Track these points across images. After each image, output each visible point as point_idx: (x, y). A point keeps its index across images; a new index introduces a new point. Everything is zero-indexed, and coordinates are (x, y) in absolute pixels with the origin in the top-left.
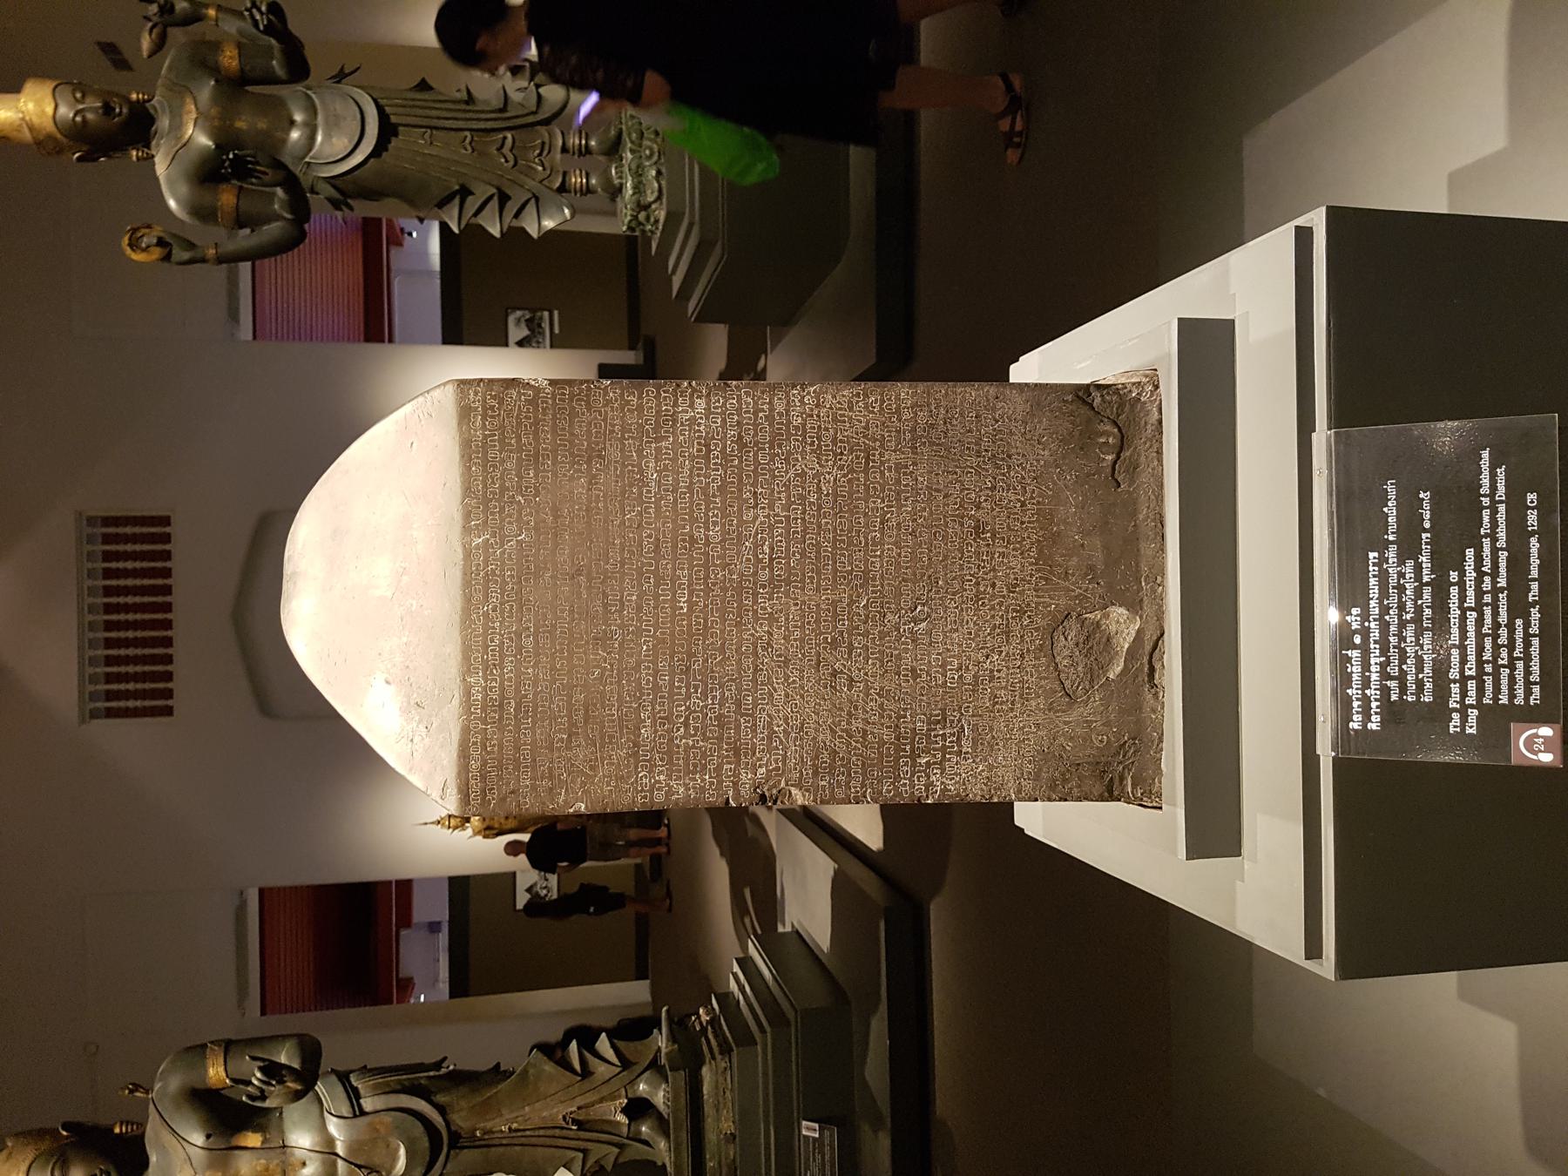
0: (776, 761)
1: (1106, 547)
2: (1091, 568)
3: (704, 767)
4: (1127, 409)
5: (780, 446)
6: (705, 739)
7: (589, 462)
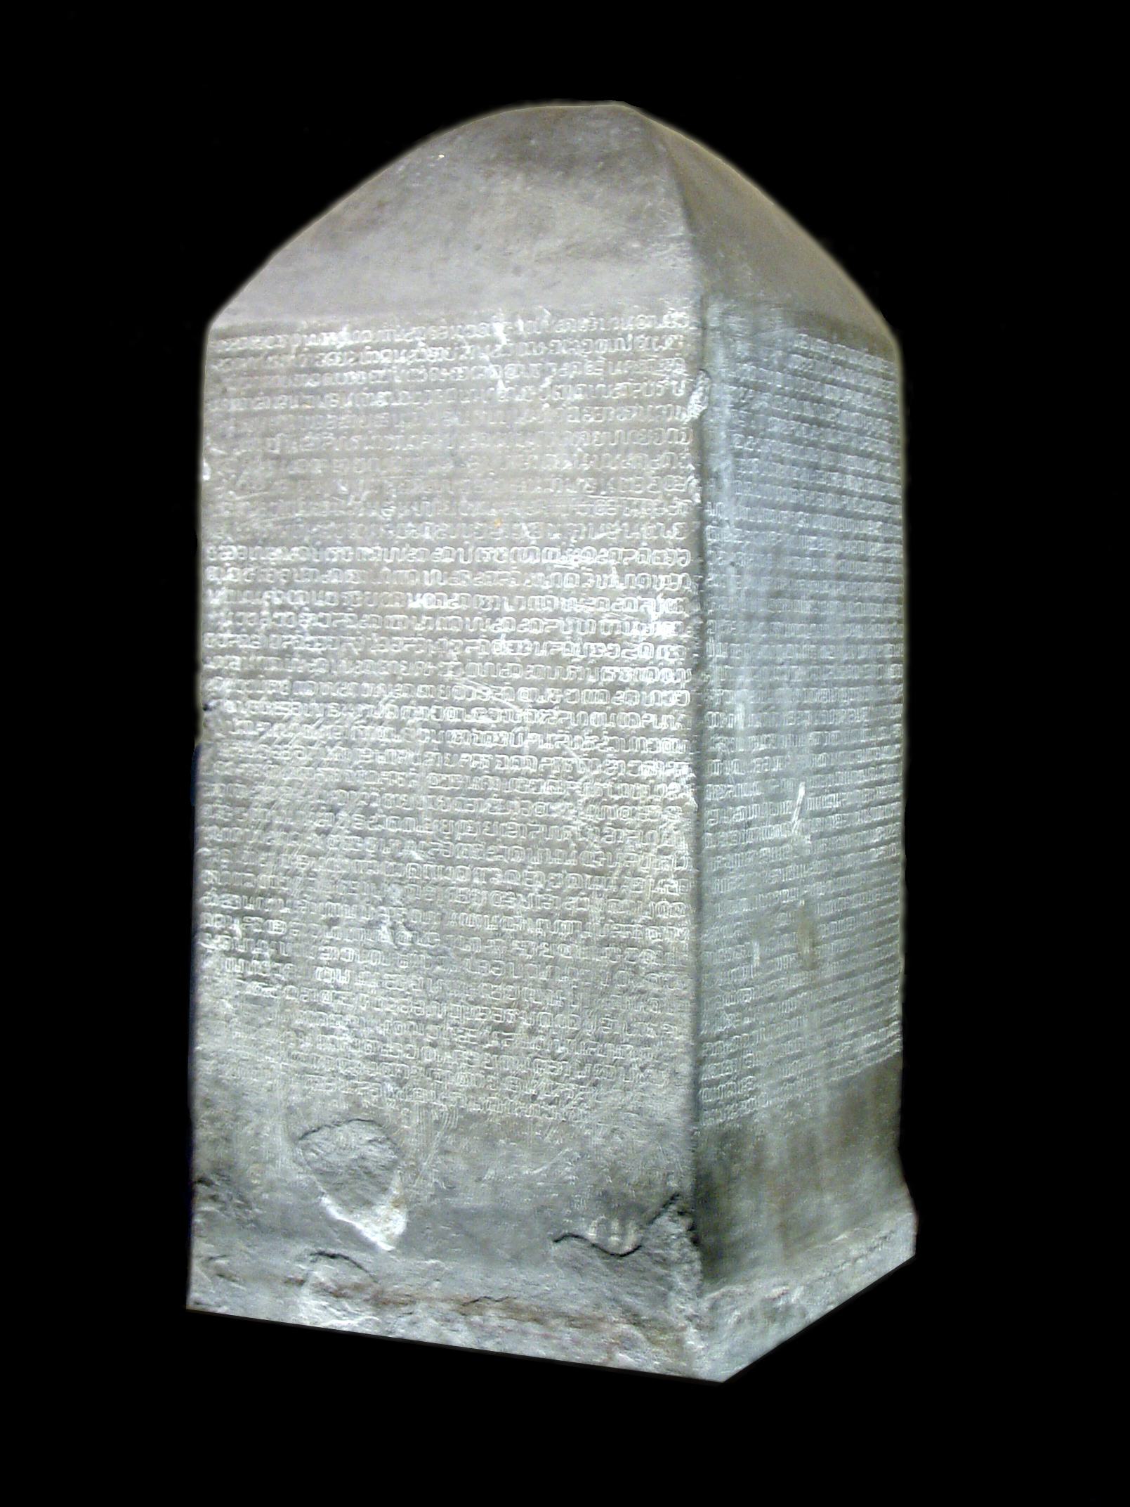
1: (476, 1214)
2: (452, 1190)
3: (237, 630)
4: (660, 1270)
5: (611, 744)
7: (591, 473)
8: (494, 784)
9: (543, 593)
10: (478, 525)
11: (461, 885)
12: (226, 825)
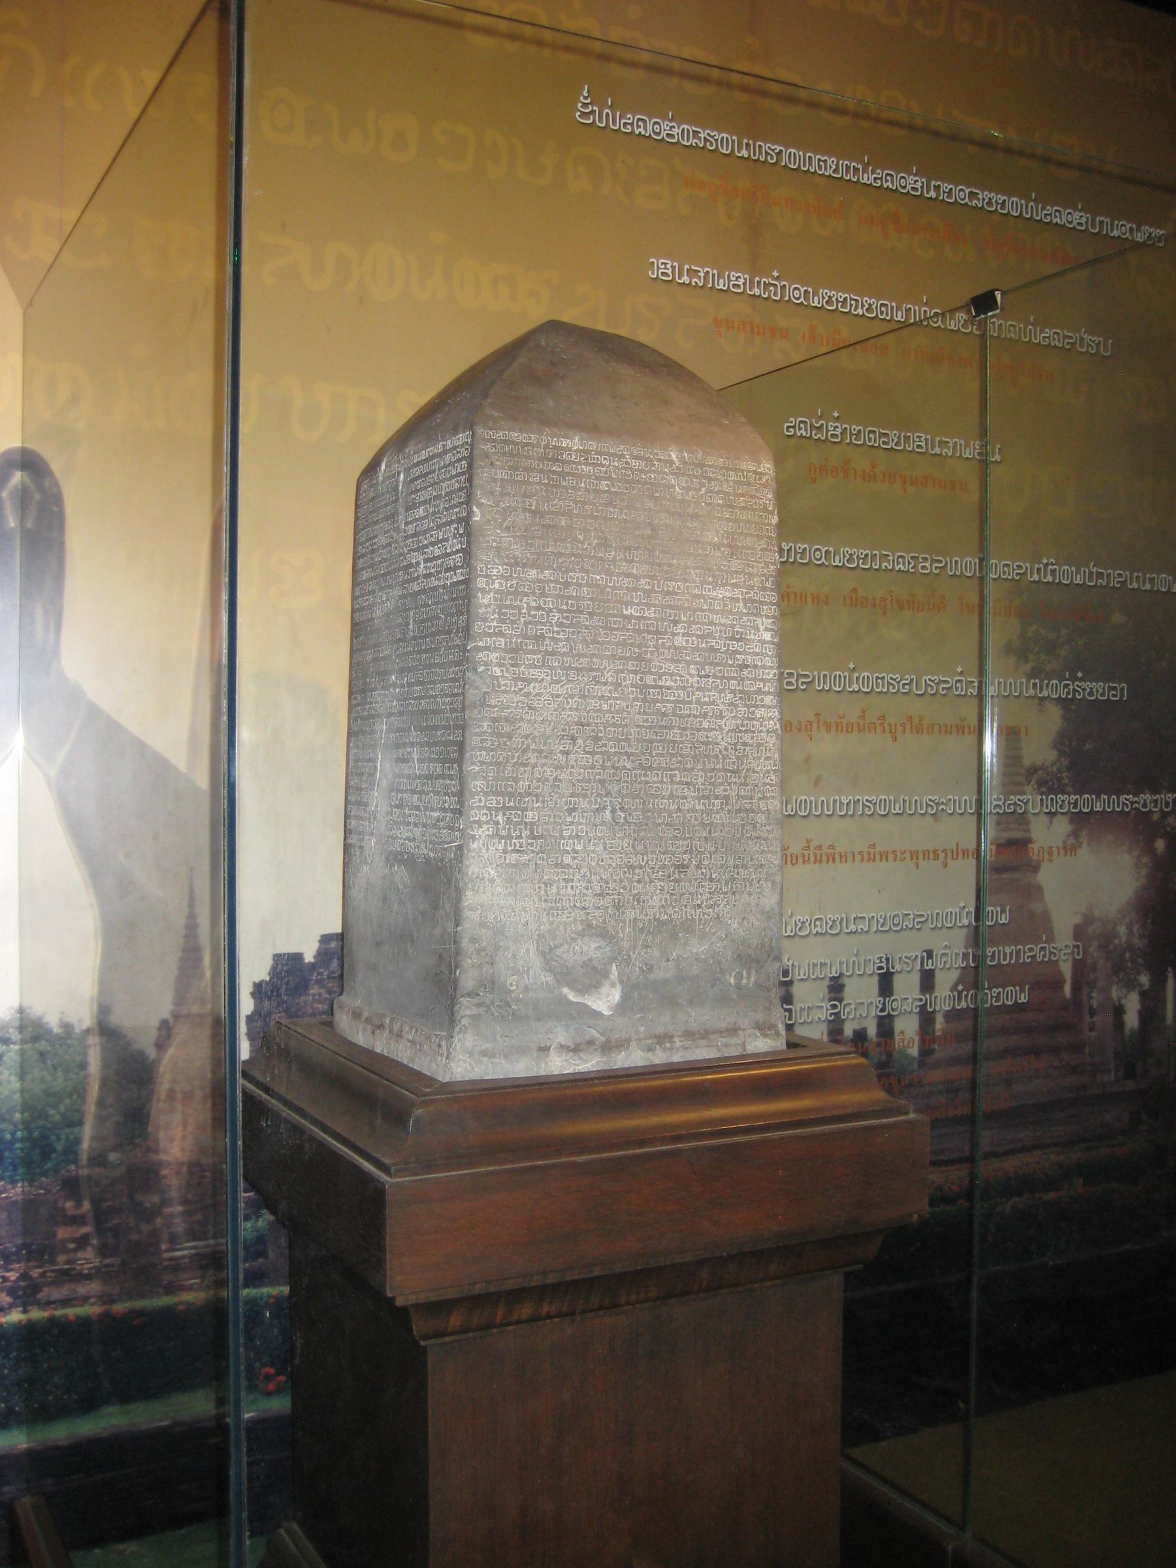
0: (505, 685)
1: (666, 981)
2: (651, 969)
3: (503, 622)
6: (526, 624)
8: (676, 721)
9: (703, 611)
10: (666, 568)
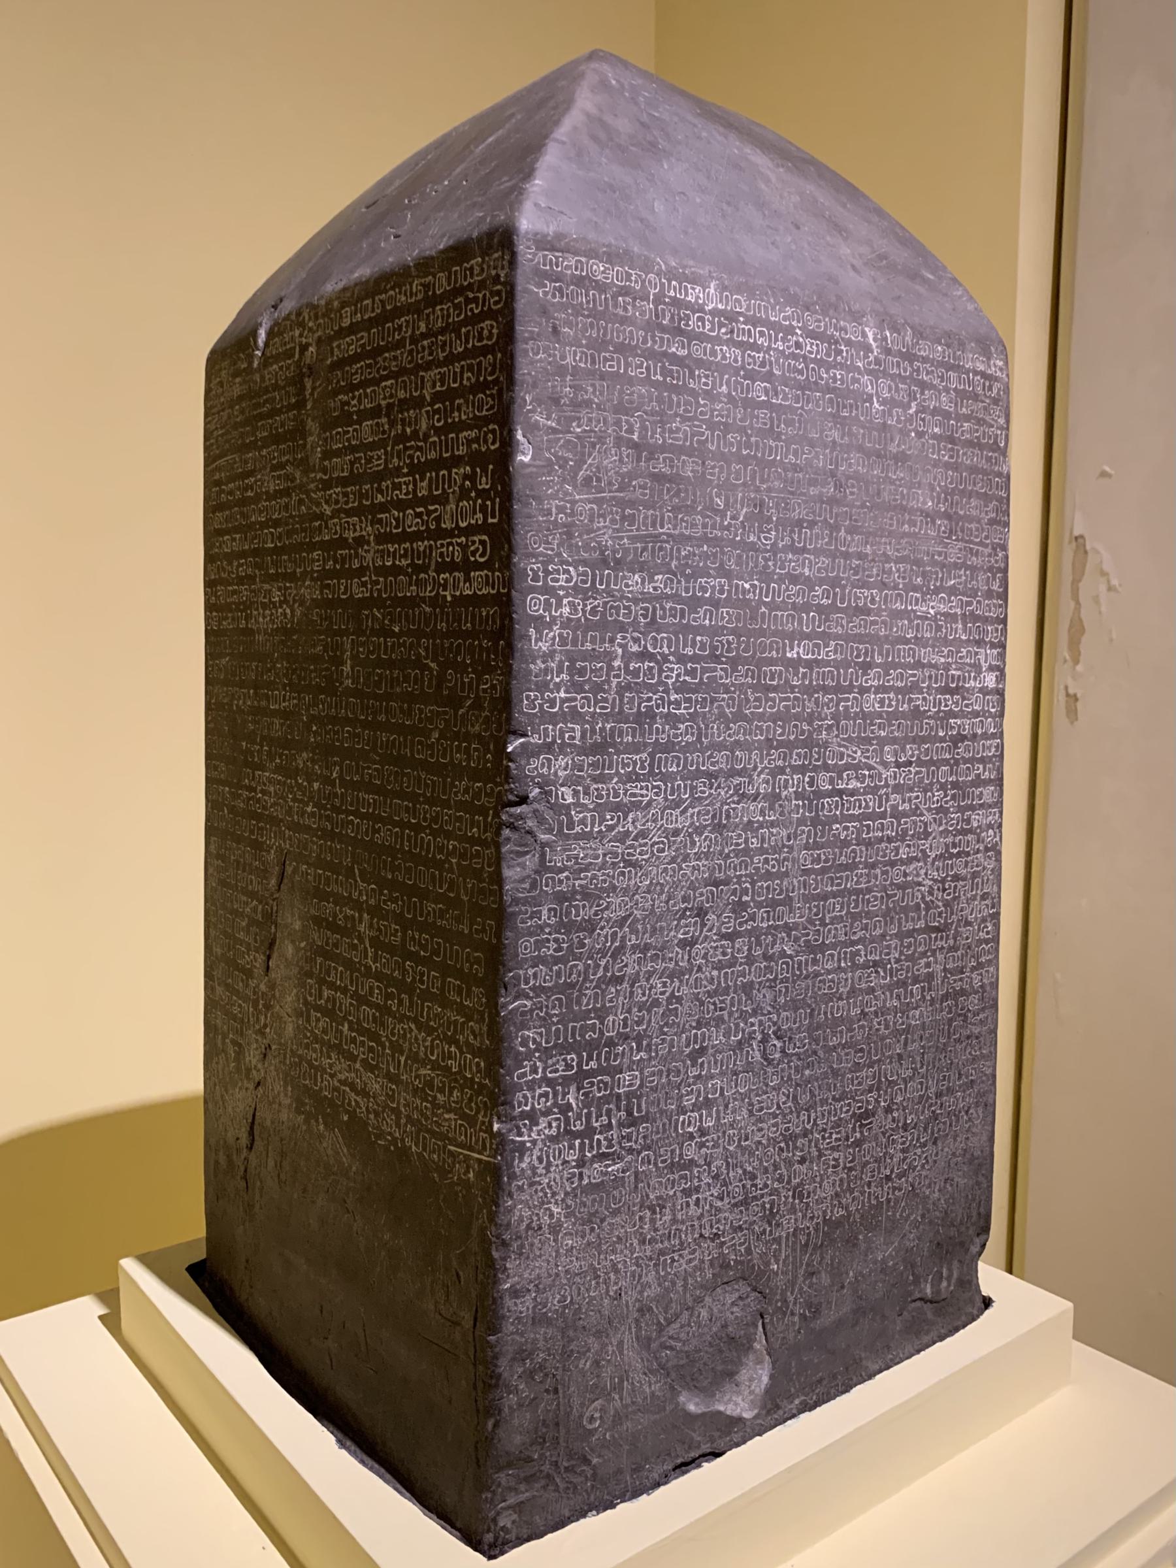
0: (583, 822)
2: (817, 1312)
3: (577, 687)
6: (621, 689)
7: (947, 516)
9: (907, 641)
11: (829, 972)
12: (557, 961)
